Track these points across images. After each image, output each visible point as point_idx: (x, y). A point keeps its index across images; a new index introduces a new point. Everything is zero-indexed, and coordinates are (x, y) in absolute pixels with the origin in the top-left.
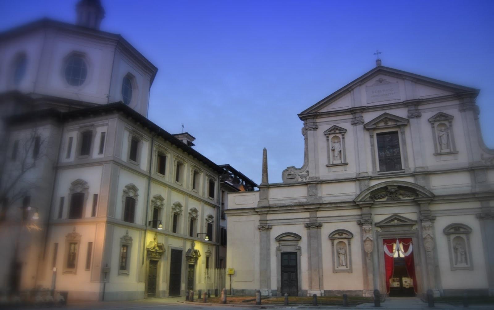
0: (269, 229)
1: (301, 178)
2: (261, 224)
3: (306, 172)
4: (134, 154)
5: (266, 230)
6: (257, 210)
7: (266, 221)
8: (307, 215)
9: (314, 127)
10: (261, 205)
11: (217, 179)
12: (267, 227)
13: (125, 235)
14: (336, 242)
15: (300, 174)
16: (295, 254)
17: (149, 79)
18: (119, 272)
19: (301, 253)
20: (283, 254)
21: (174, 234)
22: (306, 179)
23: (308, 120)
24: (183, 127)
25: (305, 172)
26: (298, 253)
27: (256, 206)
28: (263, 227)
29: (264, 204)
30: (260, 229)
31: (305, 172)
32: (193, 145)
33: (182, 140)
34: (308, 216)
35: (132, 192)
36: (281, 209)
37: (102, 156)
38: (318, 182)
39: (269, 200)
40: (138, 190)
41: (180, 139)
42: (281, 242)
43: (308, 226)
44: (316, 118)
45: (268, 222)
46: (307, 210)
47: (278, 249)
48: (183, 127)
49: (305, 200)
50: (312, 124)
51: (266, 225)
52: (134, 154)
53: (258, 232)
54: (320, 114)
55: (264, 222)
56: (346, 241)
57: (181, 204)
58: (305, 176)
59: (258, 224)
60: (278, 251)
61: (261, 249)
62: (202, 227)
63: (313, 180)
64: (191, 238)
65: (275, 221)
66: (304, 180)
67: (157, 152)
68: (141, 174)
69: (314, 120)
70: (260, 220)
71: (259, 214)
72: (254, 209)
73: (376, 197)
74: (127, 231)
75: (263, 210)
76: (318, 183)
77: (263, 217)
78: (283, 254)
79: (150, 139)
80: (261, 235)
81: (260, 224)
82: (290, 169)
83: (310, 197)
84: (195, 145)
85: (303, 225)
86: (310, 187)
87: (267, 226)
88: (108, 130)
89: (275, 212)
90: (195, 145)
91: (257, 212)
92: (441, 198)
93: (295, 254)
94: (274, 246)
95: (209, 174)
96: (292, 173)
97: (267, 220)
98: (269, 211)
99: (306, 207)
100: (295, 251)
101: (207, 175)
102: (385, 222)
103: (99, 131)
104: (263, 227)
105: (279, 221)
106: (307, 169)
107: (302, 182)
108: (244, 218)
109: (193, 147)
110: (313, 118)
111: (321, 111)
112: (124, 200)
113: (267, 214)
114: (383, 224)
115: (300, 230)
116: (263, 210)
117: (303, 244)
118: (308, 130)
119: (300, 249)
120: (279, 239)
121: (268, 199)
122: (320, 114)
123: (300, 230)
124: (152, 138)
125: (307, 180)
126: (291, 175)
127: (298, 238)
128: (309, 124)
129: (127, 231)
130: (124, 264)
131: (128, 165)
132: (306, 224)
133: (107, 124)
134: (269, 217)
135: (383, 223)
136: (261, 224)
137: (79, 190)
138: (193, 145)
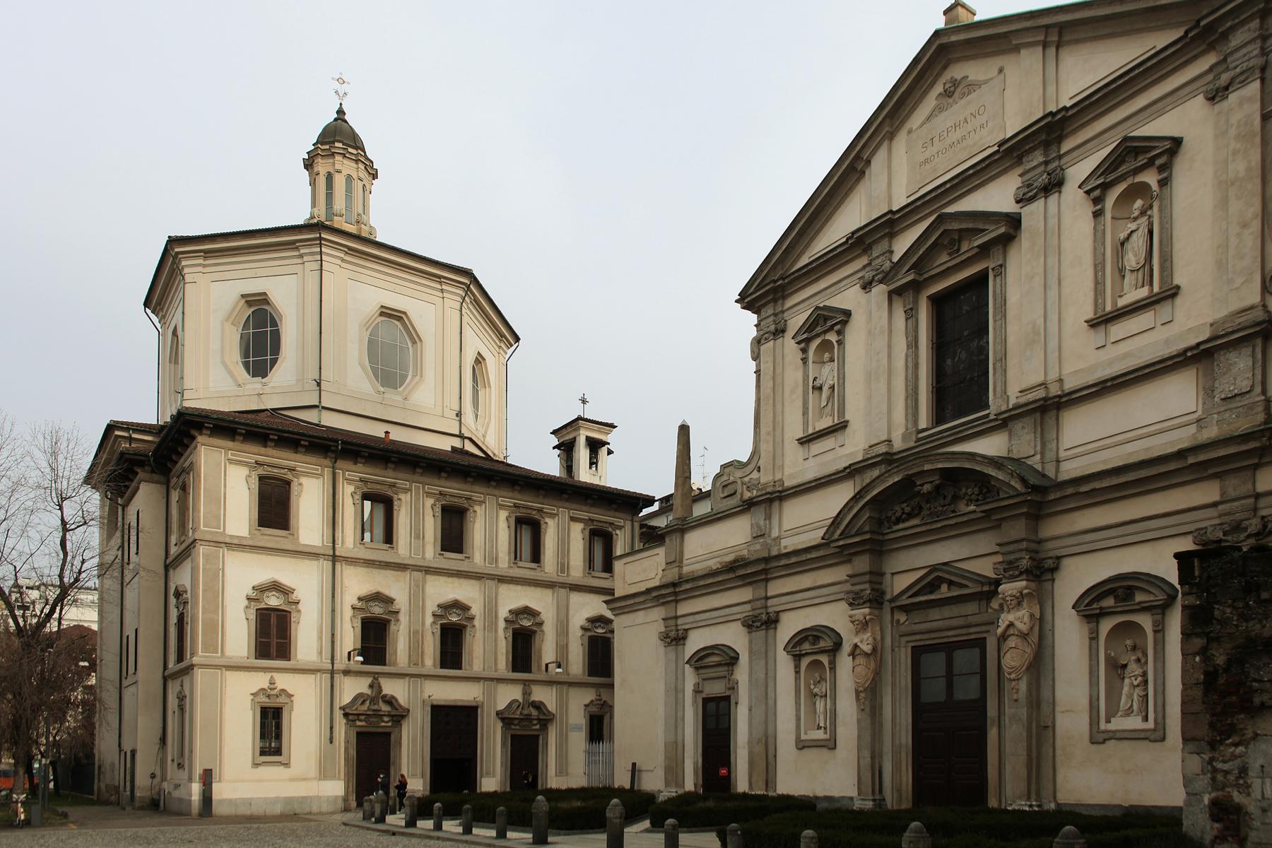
7: (674, 621)
8: (745, 594)
14: (805, 662)
34: (750, 597)
46: (747, 581)
47: (697, 691)
56: (824, 659)
62: (563, 648)
70: (663, 619)
71: (663, 604)
73: (891, 517)
79: (327, 471)
80: (666, 653)
81: (666, 627)
82: (727, 470)
85: (739, 623)
92: (1070, 491)
102: (910, 593)
105: (698, 617)
112: (253, 617)
114: (904, 601)
115: (733, 636)
117: (742, 674)
119: (733, 687)
123: (733, 636)
127: (732, 659)
129: (272, 677)
132: (742, 620)
134: (684, 608)
135: (904, 597)
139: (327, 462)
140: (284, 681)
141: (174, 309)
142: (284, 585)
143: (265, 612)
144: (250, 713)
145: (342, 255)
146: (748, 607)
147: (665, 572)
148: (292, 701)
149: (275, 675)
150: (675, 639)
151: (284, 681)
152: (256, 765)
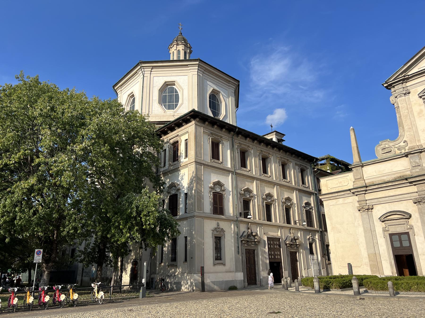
0: (370, 209)
1: (399, 149)
2: (360, 205)
3: (404, 143)
4: (215, 155)
5: (367, 210)
6: (352, 191)
7: (365, 201)
8: (414, 189)
9: (404, 92)
10: (356, 186)
11: (310, 167)
12: (367, 207)
13: (216, 227)
15: (397, 146)
16: (407, 233)
17: (233, 91)
18: (214, 262)
19: (414, 232)
20: (391, 235)
21: (269, 223)
22: (405, 150)
23: (396, 87)
24: (272, 127)
25: (402, 142)
26: (410, 233)
27: (352, 187)
28: (363, 208)
29: (360, 183)
30: (359, 210)
31: (402, 142)
32: (283, 140)
33: (272, 139)
34: (416, 190)
35: (218, 187)
36: (380, 186)
37: (187, 159)
38: (421, 150)
39: (365, 178)
40: (224, 185)
41: (269, 138)
42: (386, 222)
43: (417, 202)
44: (406, 82)
45: (367, 202)
47: (384, 230)
48: (272, 127)
49: (408, 173)
50: (402, 89)
51: (366, 205)
52: (215, 155)
53: (358, 214)
54: (410, 76)
55: (362, 202)
57: (271, 193)
58: (404, 147)
59: (357, 205)
60: (385, 232)
61: (365, 231)
63: (414, 150)
64: (288, 225)
65: (376, 200)
66: (403, 151)
67: (239, 150)
68: (227, 171)
69: (404, 85)
70: (358, 201)
71: (357, 195)
72: (350, 190)
74: (218, 223)
75: (359, 190)
76: (421, 152)
77: (361, 197)
78: (391, 235)
80: (362, 215)
83: (413, 167)
84: (285, 141)
86: (410, 157)
87: (367, 206)
88: (189, 138)
89: (374, 191)
90: (285, 141)
91: (353, 193)
93: (407, 233)
94: (379, 227)
95: (298, 163)
96: (387, 146)
97: (366, 200)
98: (366, 191)
99: (414, 184)
100: (407, 231)
101: (296, 164)
103: (183, 138)
104: (363, 208)
106: (404, 140)
107: (401, 154)
108: (341, 201)
109: (284, 143)
110: (402, 83)
111: (409, 74)
113: (365, 194)
116: (359, 190)
118: (398, 97)
119: (412, 228)
120: (384, 219)
121: (363, 178)
122: (410, 76)
124: (232, 138)
125: (407, 151)
126: (386, 149)
128: (398, 90)
129: (218, 223)
130: (219, 255)
131: (209, 164)
133: (187, 132)
134: (368, 196)
136: (360, 205)
137: (173, 192)
138: (283, 140)
139: (230, 136)
140: (223, 225)
141: (130, 87)
142: (221, 183)
143: (215, 194)
144: (211, 239)
145: (203, 71)
146: (417, 194)
147: (355, 183)
148: (224, 234)
149: (219, 222)
150: (367, 209)
151: (223, 225)
152: (214, 265)
